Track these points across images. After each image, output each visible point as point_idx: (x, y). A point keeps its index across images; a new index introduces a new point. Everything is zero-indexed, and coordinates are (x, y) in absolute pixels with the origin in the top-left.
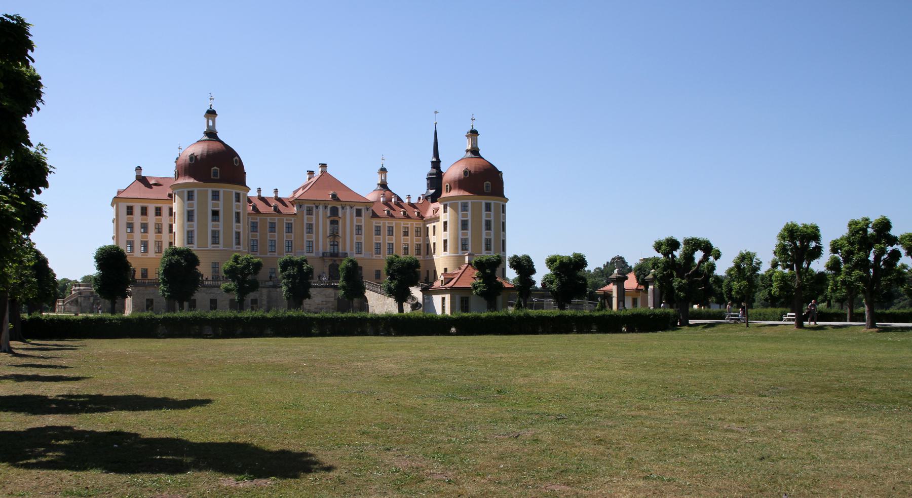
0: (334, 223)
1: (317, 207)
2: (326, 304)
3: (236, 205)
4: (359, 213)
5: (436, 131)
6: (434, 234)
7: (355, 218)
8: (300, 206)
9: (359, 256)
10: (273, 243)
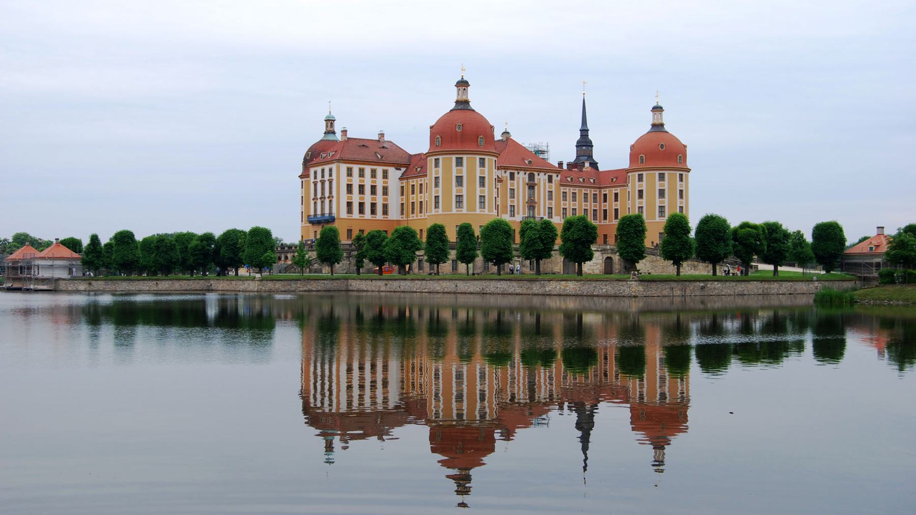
0: (531, 187)
1: (518, 173)
2: (596, 266)
3: (680, 184)
5: (584, 100)
9: (513, 219)
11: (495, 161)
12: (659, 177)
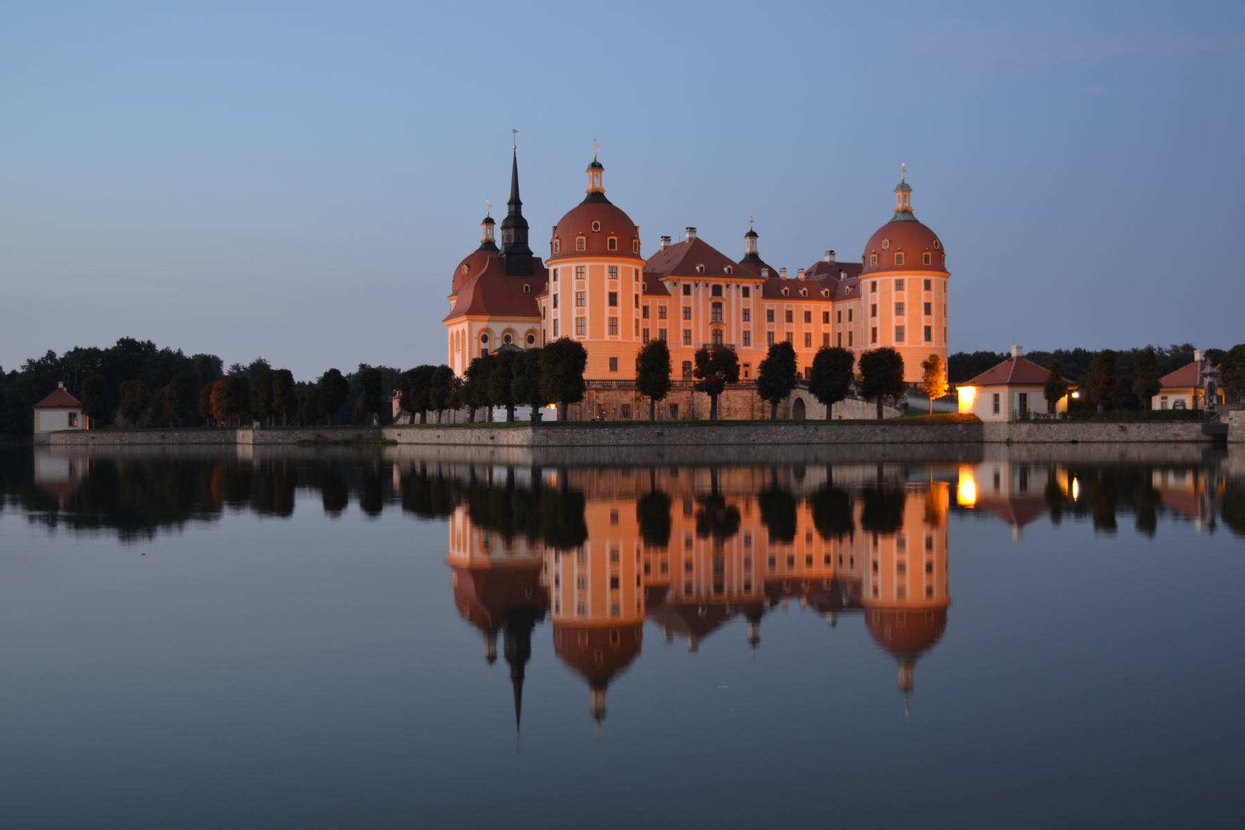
0: (717, 306)
1: (697, 285)
4: (746, 292)
6: (850, 319)
7: (742, 299)
8: (675, 284)
10: (579, 330)
11: (637, 271)
12: (897, 285)
